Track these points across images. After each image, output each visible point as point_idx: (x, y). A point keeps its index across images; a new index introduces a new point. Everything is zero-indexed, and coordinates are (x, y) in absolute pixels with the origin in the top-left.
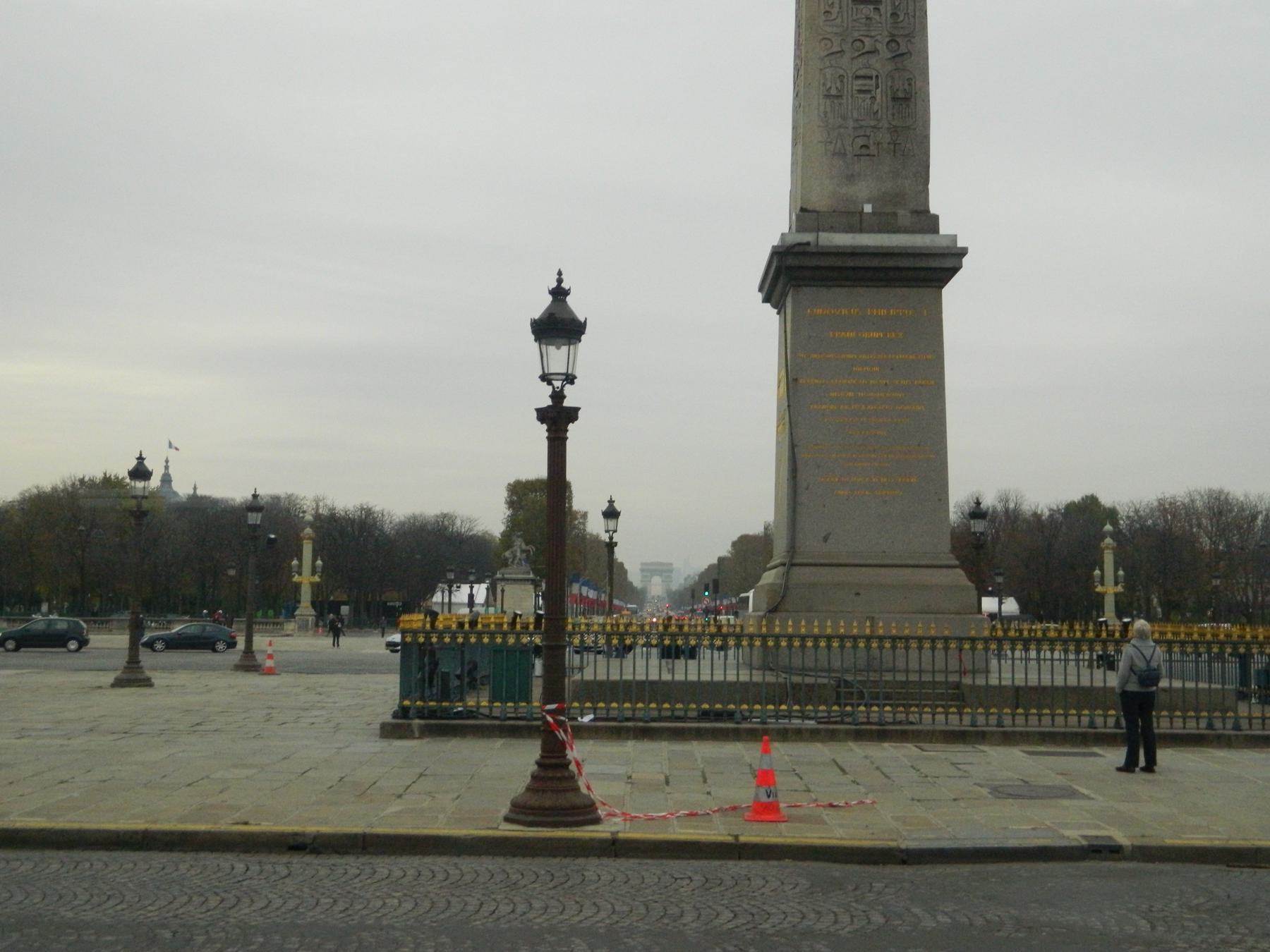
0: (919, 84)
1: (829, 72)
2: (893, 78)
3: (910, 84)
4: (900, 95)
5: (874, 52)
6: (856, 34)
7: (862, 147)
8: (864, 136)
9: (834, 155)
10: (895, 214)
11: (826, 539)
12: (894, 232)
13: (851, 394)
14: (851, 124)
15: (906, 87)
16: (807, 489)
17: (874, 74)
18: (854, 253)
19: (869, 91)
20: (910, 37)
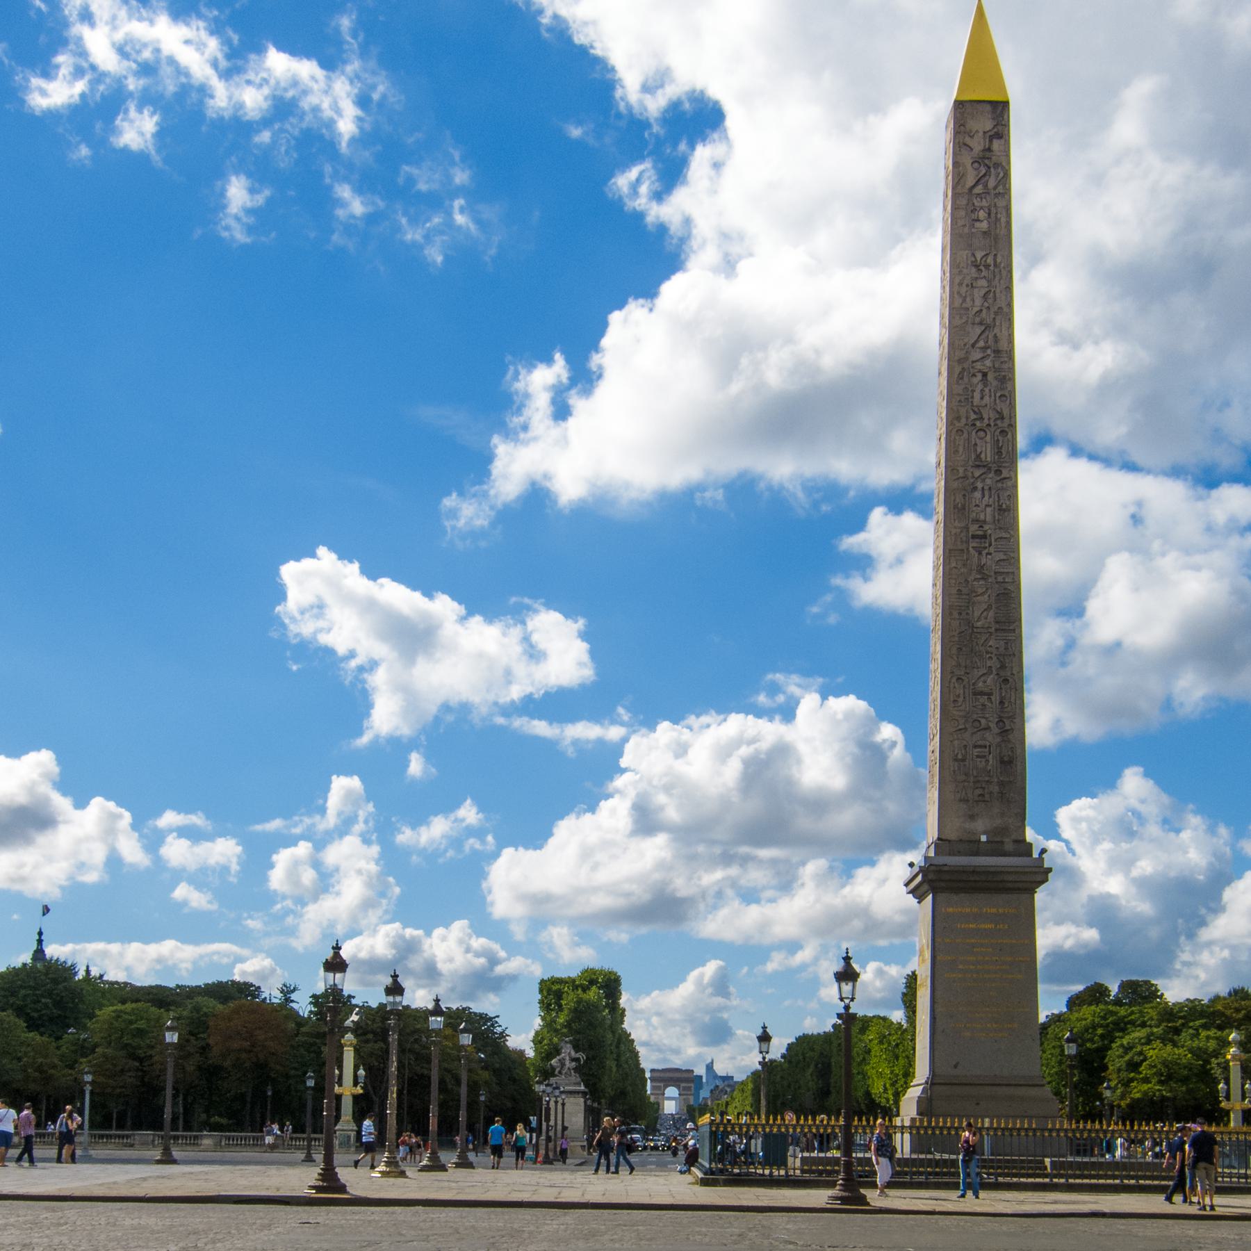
0: (1019, 751)
1: (956, 742)
2: (1000, 746)
3: (1012, 751)
4: (1006, 759)
5: (988, 728)
6: (975, 716)
7: (980, 795)
8: (981, 788)
9: (961, 800)
10: (1002, 842)
11: (955, 1066)
12: (1001, 856)
13: (971, 967)
14: (972, 779)
15: (1010, 753)
16: (943, 1031)
17: (988, 744)
18: (975, 871)
19: (985, 756)
20: (1012, 718)
